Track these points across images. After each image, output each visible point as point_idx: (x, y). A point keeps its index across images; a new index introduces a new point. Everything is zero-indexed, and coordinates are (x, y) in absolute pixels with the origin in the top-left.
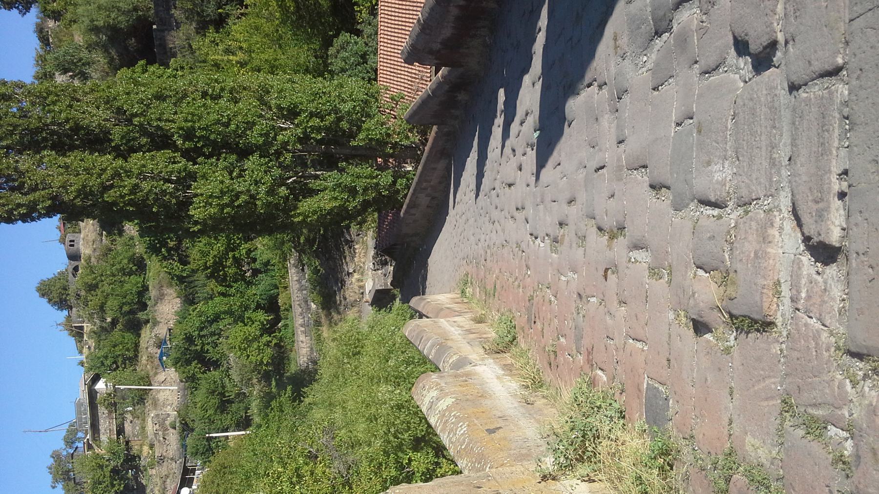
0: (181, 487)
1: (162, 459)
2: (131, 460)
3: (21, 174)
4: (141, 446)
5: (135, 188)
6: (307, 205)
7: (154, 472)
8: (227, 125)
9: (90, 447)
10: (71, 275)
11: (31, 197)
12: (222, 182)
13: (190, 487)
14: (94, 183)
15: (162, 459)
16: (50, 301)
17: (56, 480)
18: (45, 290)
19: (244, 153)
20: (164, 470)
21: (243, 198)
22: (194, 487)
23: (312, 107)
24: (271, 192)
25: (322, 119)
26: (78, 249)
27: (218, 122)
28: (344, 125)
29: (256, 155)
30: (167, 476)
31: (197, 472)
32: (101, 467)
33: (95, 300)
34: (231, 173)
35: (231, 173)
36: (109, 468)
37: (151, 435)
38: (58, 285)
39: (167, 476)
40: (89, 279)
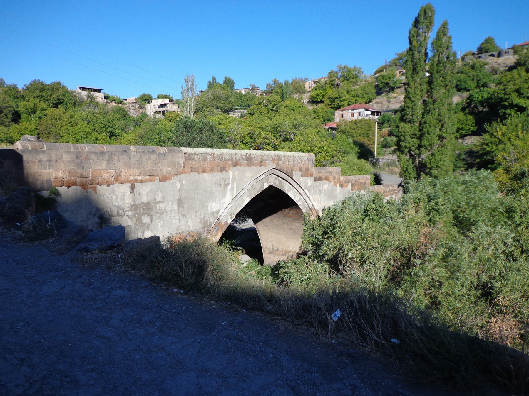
0: (371, 111)
1: (389, 102)
2: (392, 89)
3: (417, 73)
4: (397, 93)
5: (408, 107)
6: (406, 158)
7: (385, 98)
8: (428, 134)
9: (400, 72)
10: (490, 53)
11: (409, 77)
12: (408, 132)
13: (371, 114)
14: (410, 95)
15: (389, 102)
16: (483, 43)
17: (399, 55)
18: (489, 41)
19: (420, 138)
20: (385, 103)
21: (402, 138)
22: (371, 116)
23: (433, 160)
24: (406, 147)
25: (430, 163)
26: (503, 56)
27: (428, 131)
28: (427, 170)
29: (419, 143)
30: (382, 104)
31: (377, 117)
32: (390, 78)
33: (467, 69)
34: (413, 135)
35: (413, 135)
36: (389, 82)
37: (399, 97)
38: (490, 47)
39: (382, 104)
40: (478, 65)
